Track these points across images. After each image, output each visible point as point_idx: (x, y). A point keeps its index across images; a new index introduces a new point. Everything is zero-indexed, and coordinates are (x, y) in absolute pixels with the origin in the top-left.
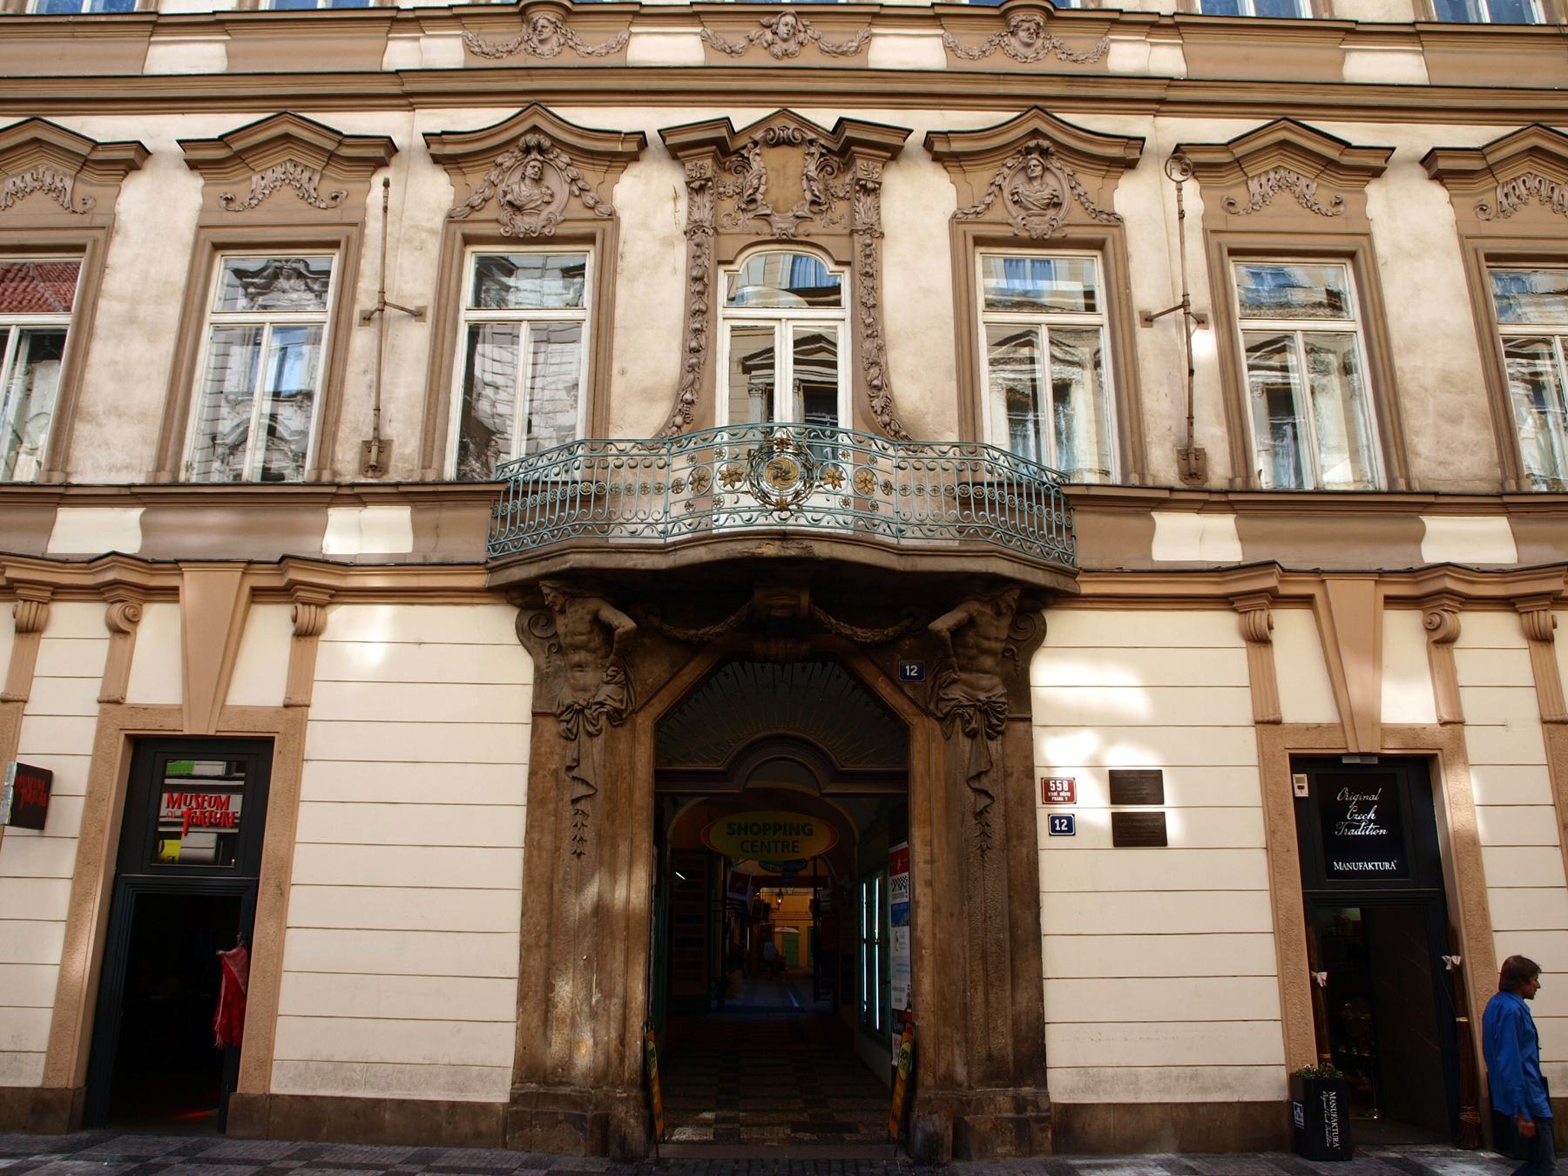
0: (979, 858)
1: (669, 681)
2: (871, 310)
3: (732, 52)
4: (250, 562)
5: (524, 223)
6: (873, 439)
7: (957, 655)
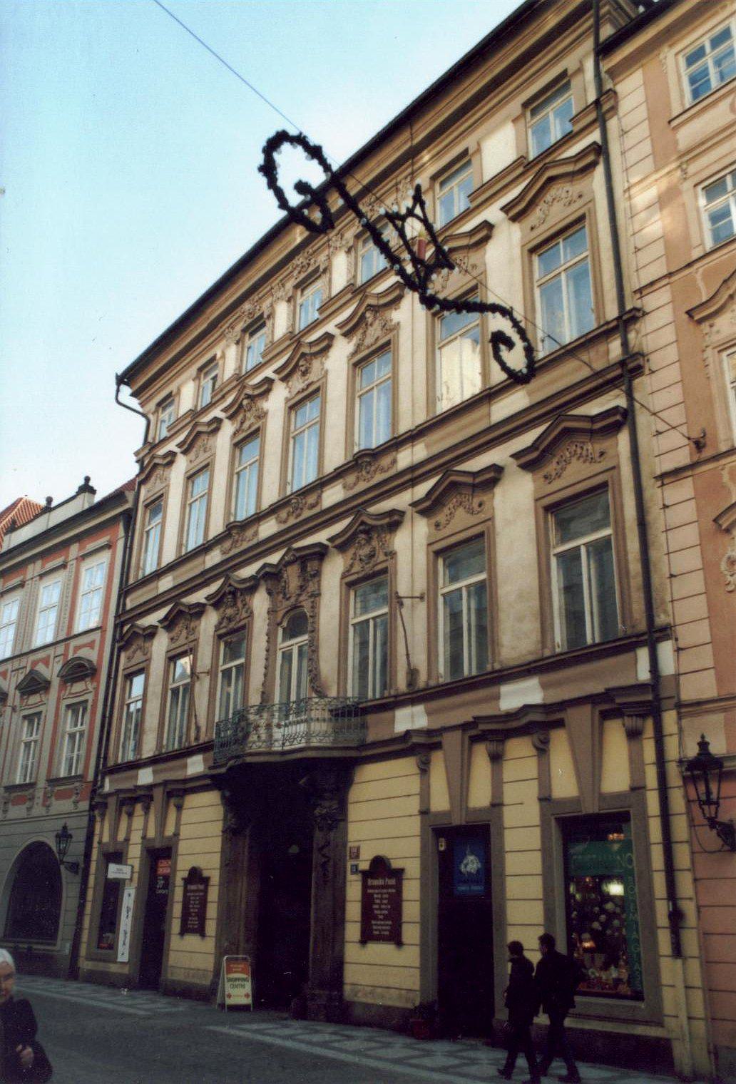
5: (232, 625)
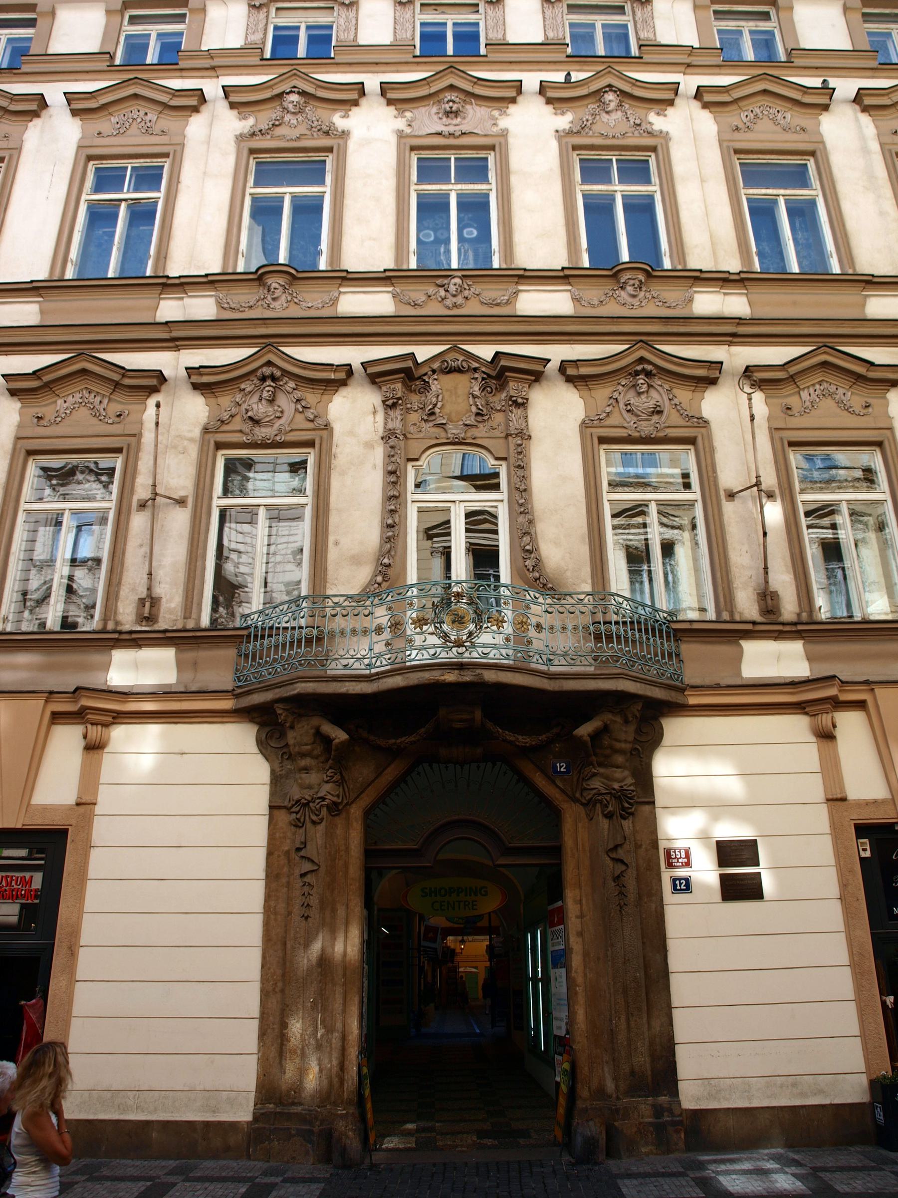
0: (618, 912)
1: (373, 781)
2: (523, 494)
3: (416, 305)
4: (51, 693)
5: (262, 433)
6: (527, 591)
7: (596, 755)
